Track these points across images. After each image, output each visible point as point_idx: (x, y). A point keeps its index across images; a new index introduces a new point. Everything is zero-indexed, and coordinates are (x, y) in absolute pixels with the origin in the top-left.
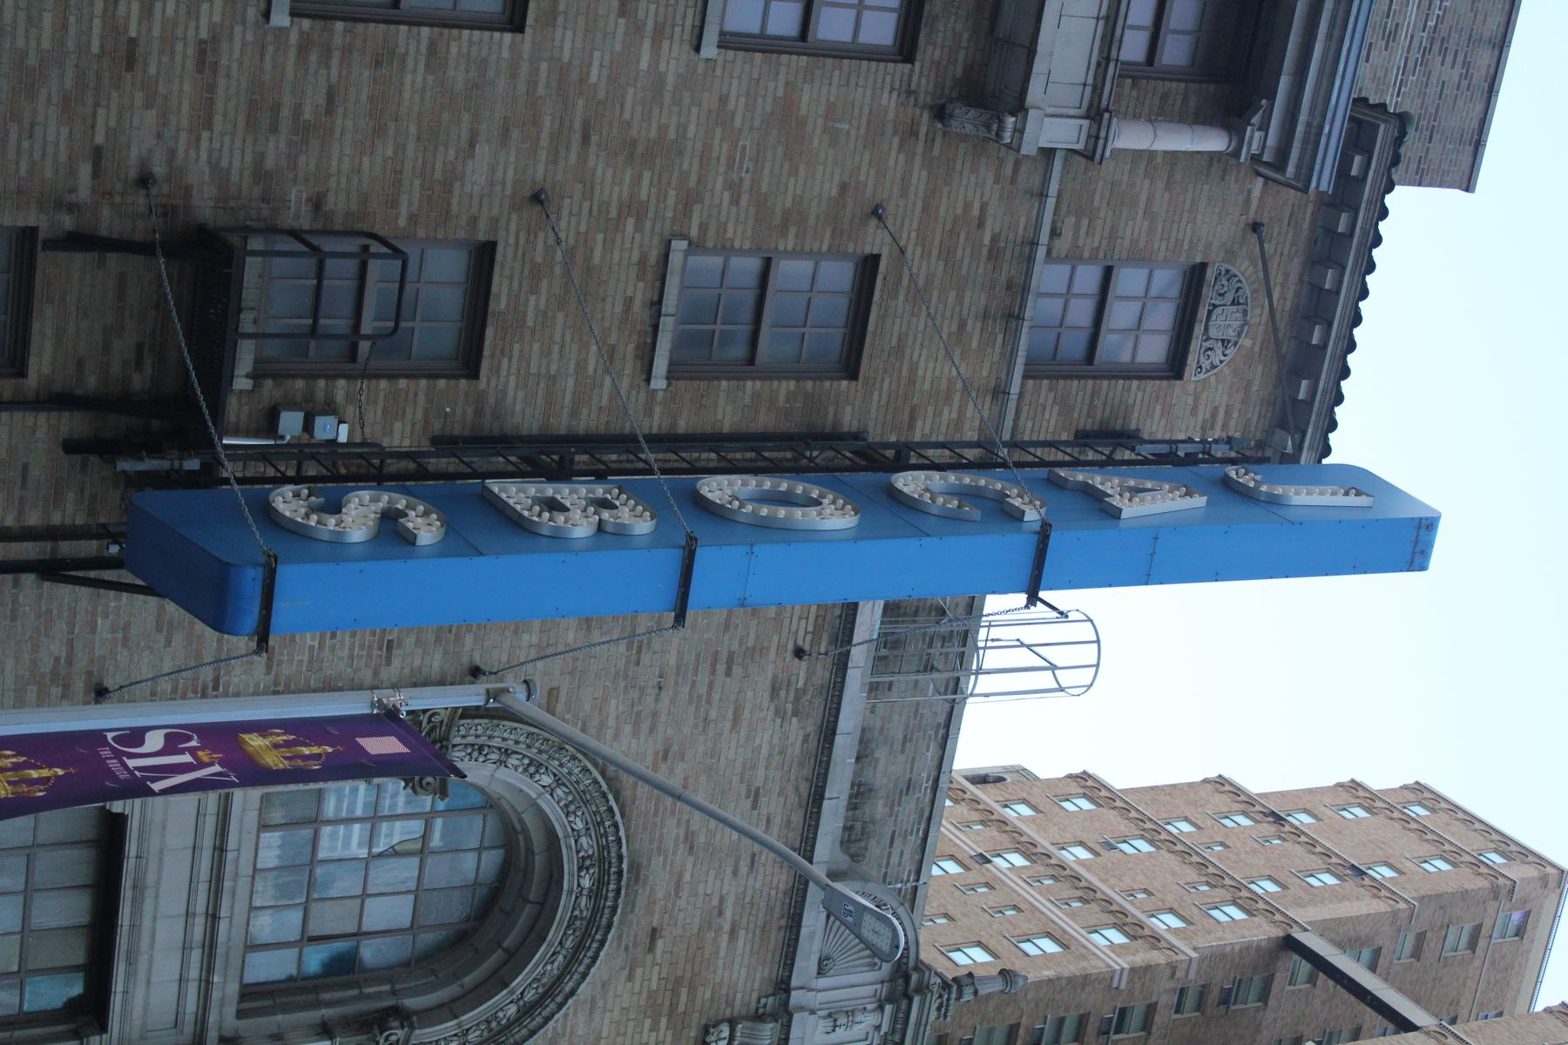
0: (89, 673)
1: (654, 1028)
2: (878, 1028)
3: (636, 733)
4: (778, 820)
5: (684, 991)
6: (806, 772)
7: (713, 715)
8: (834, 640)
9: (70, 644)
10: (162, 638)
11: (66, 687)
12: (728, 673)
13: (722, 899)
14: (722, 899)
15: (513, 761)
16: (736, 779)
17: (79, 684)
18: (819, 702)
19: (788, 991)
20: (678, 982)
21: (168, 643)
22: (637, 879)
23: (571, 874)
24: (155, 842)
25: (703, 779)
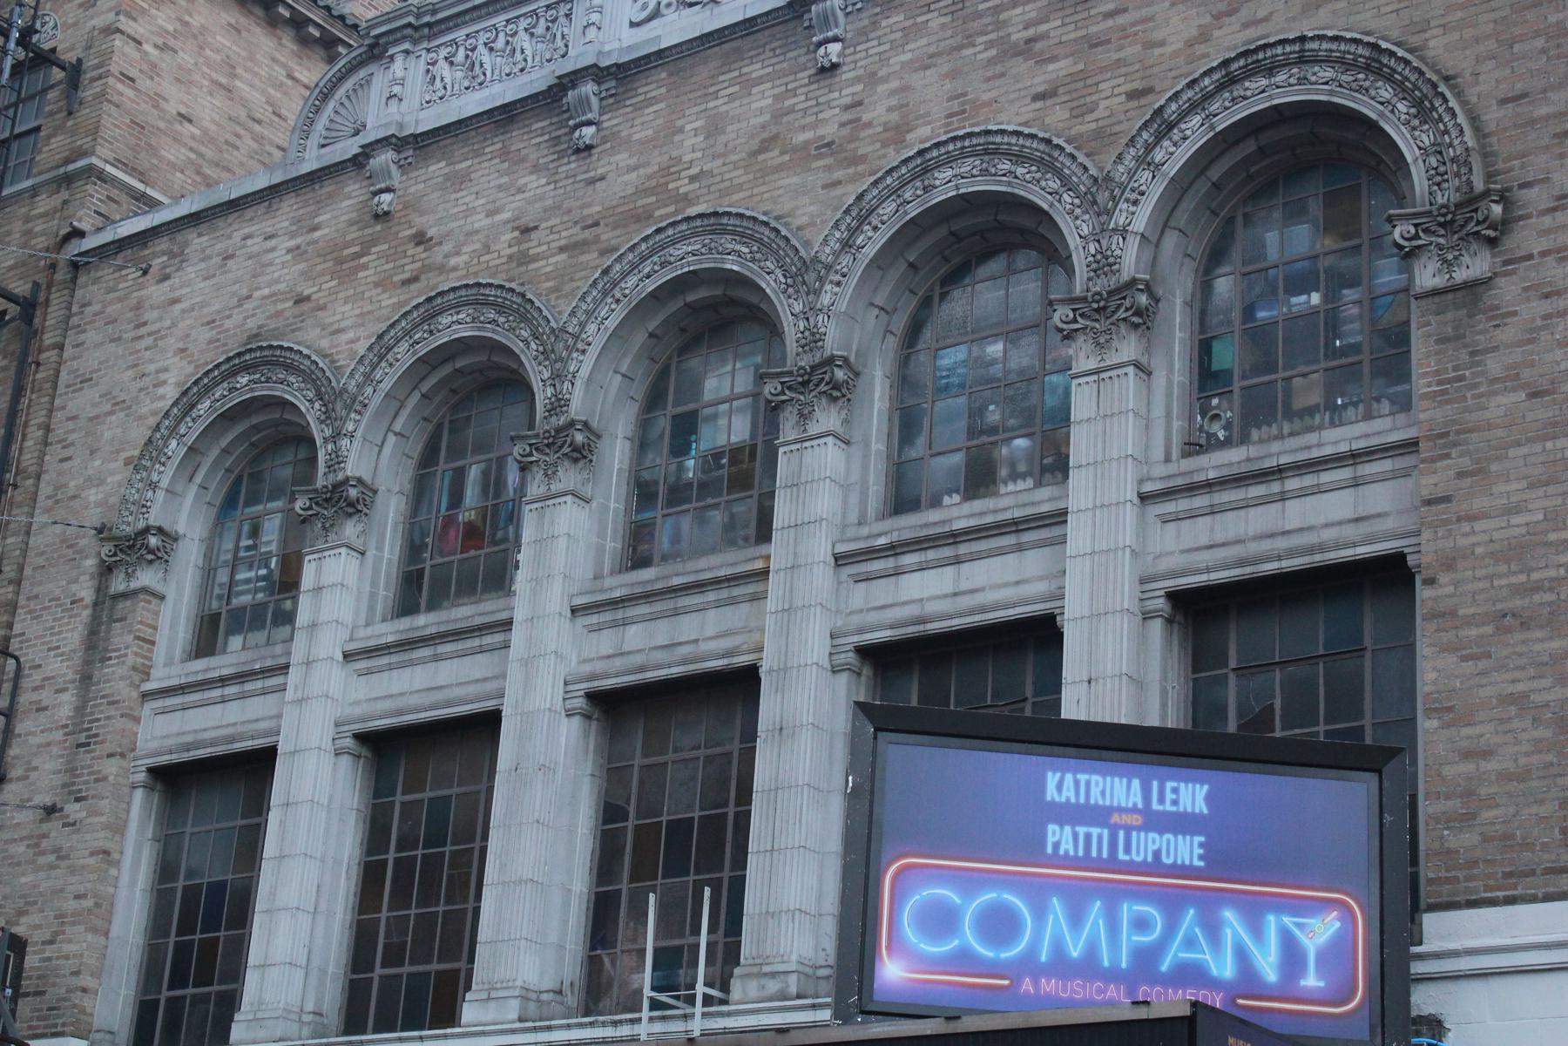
0: (42, 821)
1: (365, 267)
2: (407, 52)
3: (165, 382)
4: (246, 231)
5: (346, 252)
6: (221, 223)
7: (168, 323)
8: (145, 245)
9: (22, 839)
10: (33, 775)
11: (45, 836)
12: (145, 324)
13: (289, 251)
14: (289, 251)
15: (155, 477)
16: (214, 281)
17: (45, 826)
18: (180, 237)
19: (355, 156)
20: (340, 261)
21: (36, 768)
22: (257, 335)
23: (241, 395)
24: (171, 742)
25: (205, 310)
